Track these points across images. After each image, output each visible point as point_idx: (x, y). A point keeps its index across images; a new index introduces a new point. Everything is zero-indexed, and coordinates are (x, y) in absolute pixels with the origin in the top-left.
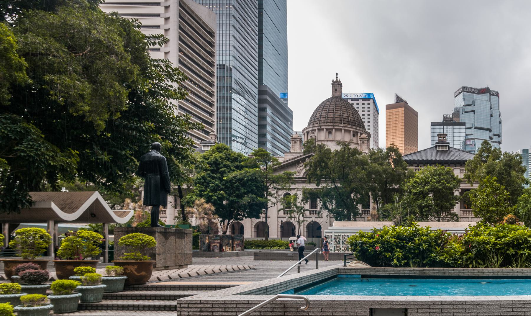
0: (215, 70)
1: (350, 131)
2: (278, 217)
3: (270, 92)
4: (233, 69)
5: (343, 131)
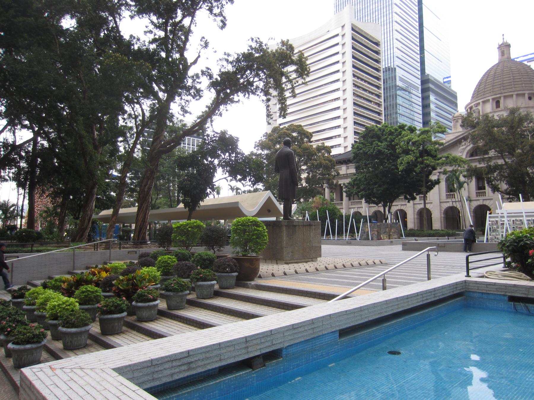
0: (381, 74)
1: (524, 94)
2: (440, 202)
3: (433, 79)
4: (397, 69)
5: (514, 96)
